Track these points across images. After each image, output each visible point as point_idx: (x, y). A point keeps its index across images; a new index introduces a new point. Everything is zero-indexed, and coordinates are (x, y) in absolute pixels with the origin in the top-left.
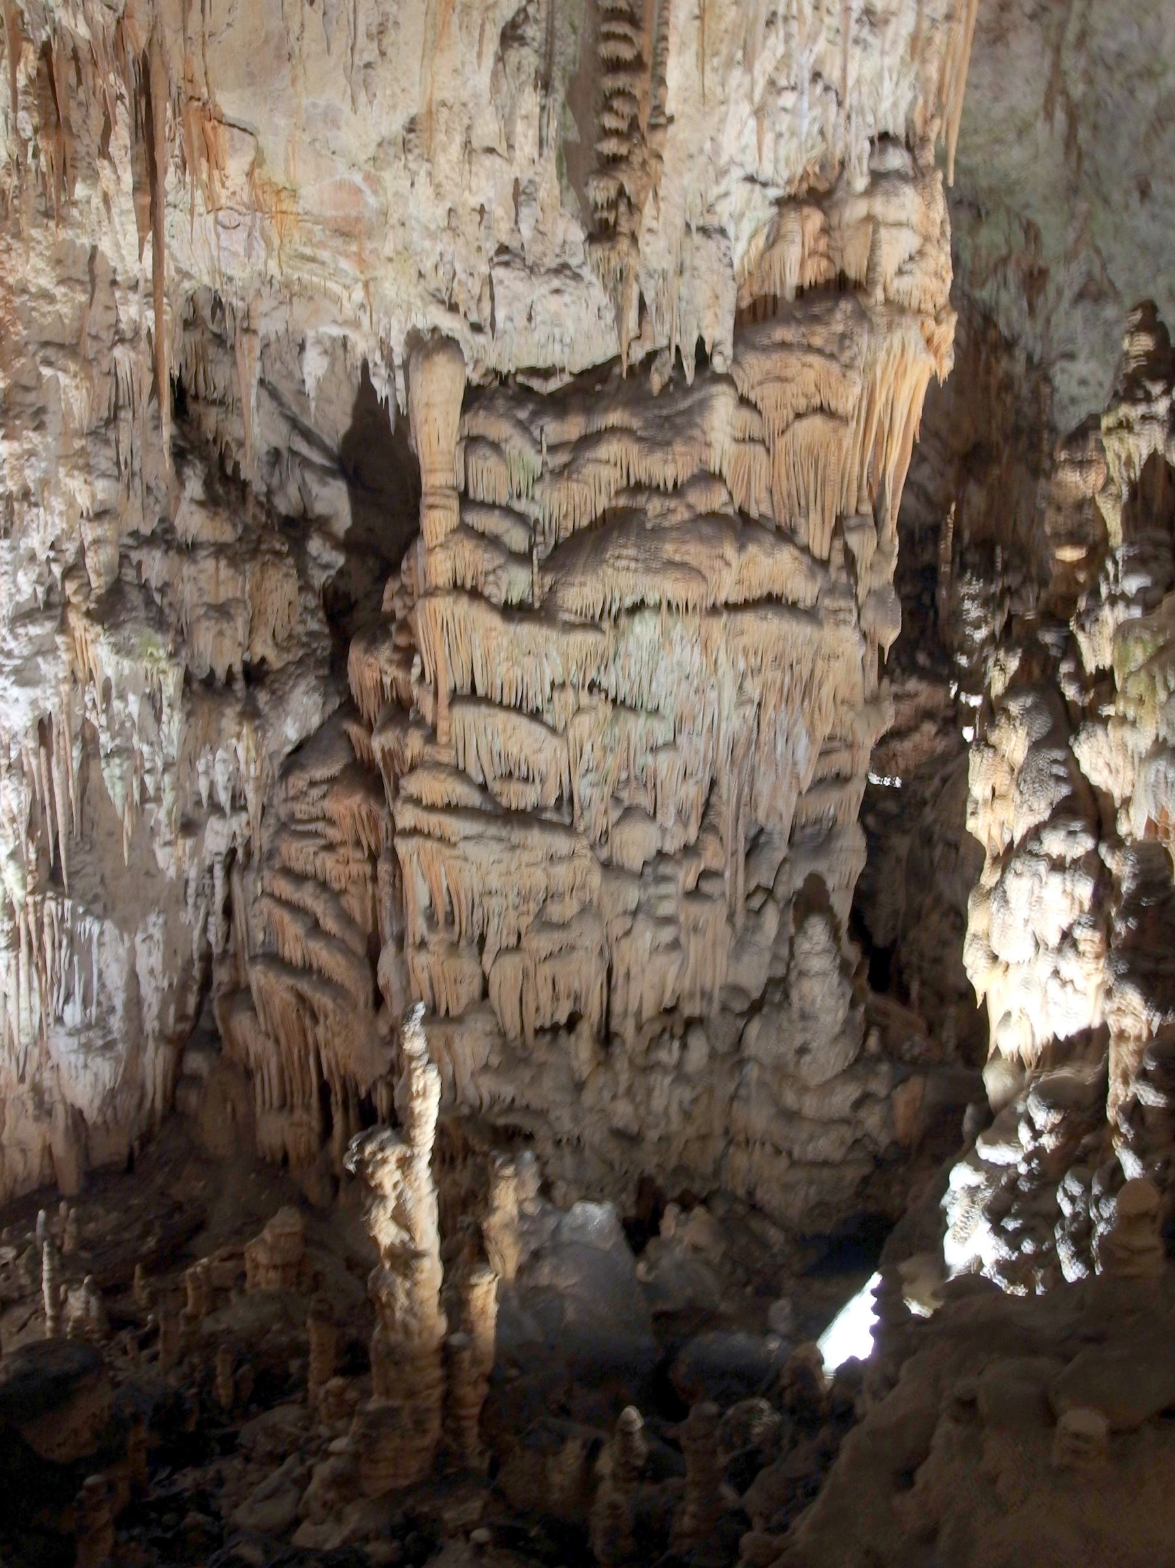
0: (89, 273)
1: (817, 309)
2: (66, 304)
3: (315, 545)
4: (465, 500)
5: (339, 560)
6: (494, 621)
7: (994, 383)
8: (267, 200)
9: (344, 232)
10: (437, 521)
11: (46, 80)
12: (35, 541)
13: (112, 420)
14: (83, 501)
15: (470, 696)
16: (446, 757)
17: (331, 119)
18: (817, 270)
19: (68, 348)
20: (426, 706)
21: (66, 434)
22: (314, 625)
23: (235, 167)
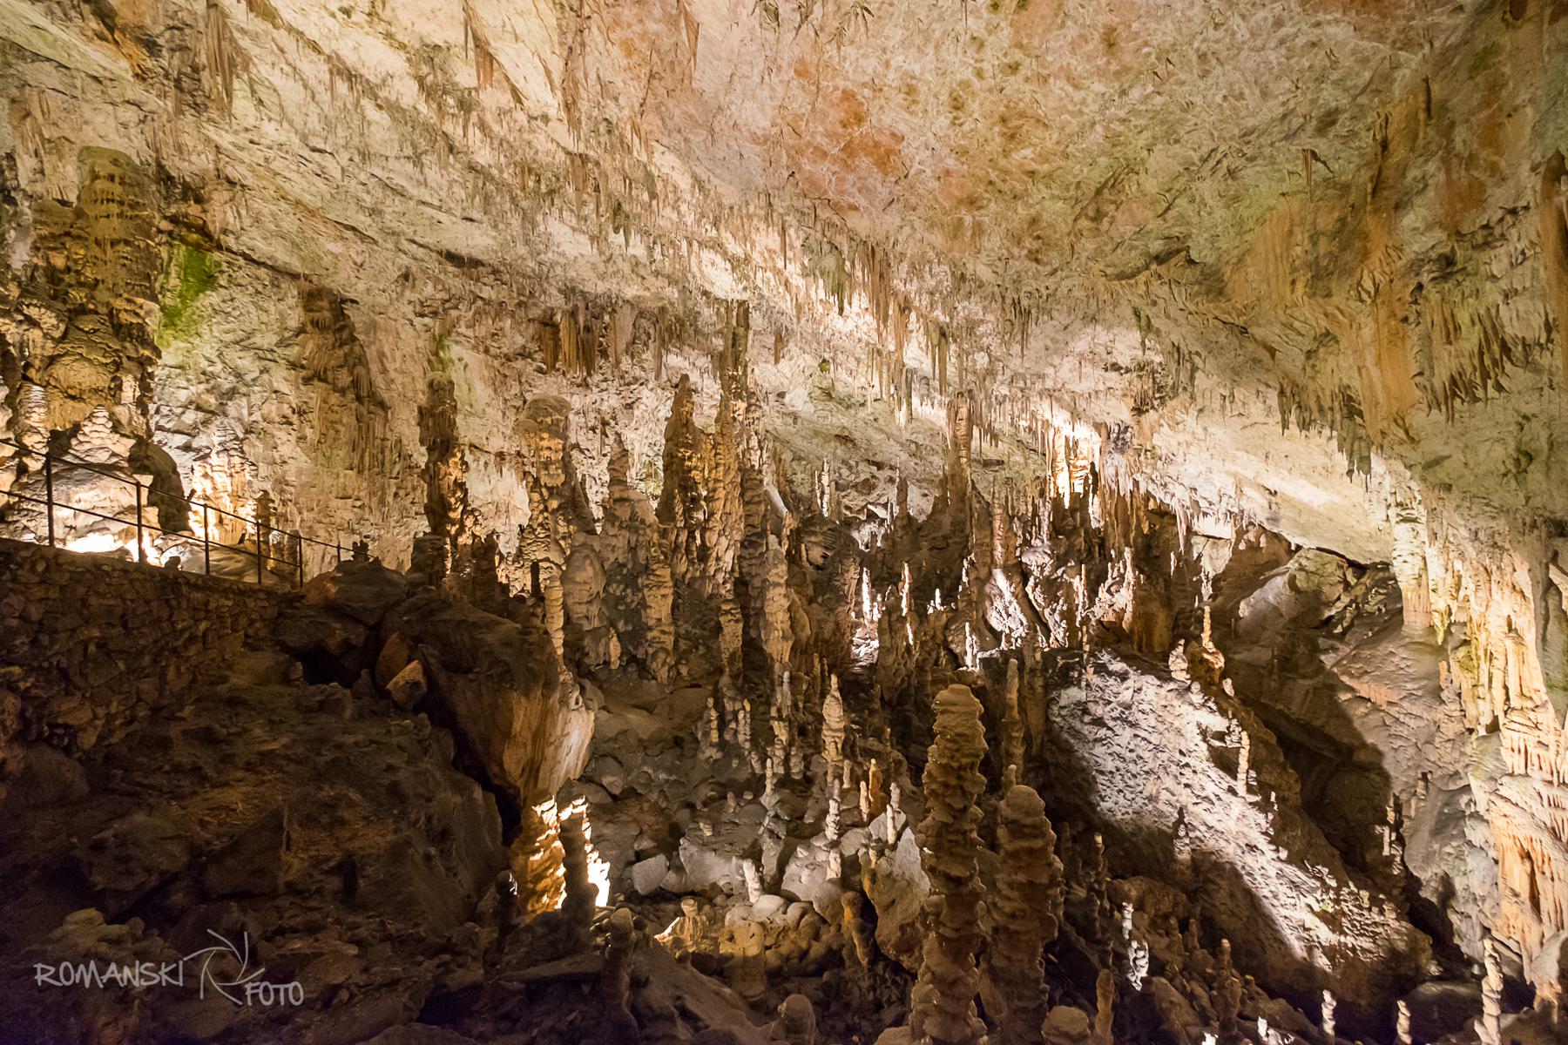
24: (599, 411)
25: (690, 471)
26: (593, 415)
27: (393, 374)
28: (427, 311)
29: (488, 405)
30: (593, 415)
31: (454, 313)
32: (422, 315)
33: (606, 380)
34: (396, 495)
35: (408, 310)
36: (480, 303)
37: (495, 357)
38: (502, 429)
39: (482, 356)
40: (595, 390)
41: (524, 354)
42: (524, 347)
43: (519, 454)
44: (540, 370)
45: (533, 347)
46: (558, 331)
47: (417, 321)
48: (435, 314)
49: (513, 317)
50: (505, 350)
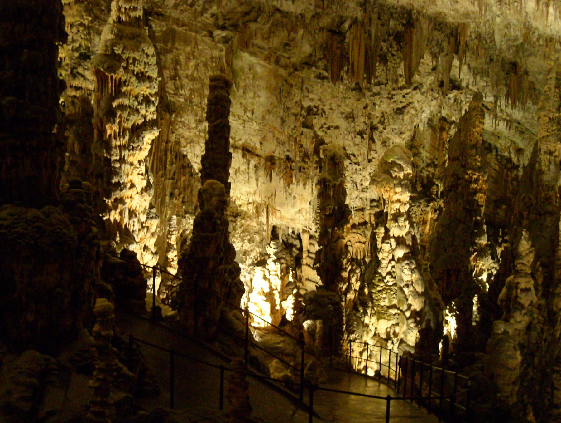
0: (261, 224)
1: (360, 227)
2: (257, 228)
3: (294, 249)
4: (309, 251)
5: (298, 252)
6: (311, 270)
7: (509, 179)
8: (281, 218)
9: (292, 220)
10: (304, 255)
11: (257, 207)
12: (252, 256)
13: (262, 241)
14: (258, 251)
15: (308, 280)
16: (304, 288)
17: (289, 210)
18: (362, 221)
19: (257, 233)
20: (303, 280)
21: (256, 243)
22: (292, 263)
23: (278, 214)
24: (369, 116)
25: (475, 192)
26: (362, 119)
27: (185, 81)
28: (228, 23)
29: (269, 112)
30: (362, 119)
31: (253, 26)
32: (223, 28)
33: (379, 84)
34: (172, 195)
35: (211, 21)
36: (278, 16)
37: (286, 67)
38: (277, 134)
39: (272, 66)
40: (368, 94)
41: (308, 63)
42: (311, 55)
43: (288, 158)
44: (320, 77)
45: (319, 54)
46: (345, 38)
47: (218, 33)
48: (235, 26)
49: (305, 27)
50: (294, 60)
